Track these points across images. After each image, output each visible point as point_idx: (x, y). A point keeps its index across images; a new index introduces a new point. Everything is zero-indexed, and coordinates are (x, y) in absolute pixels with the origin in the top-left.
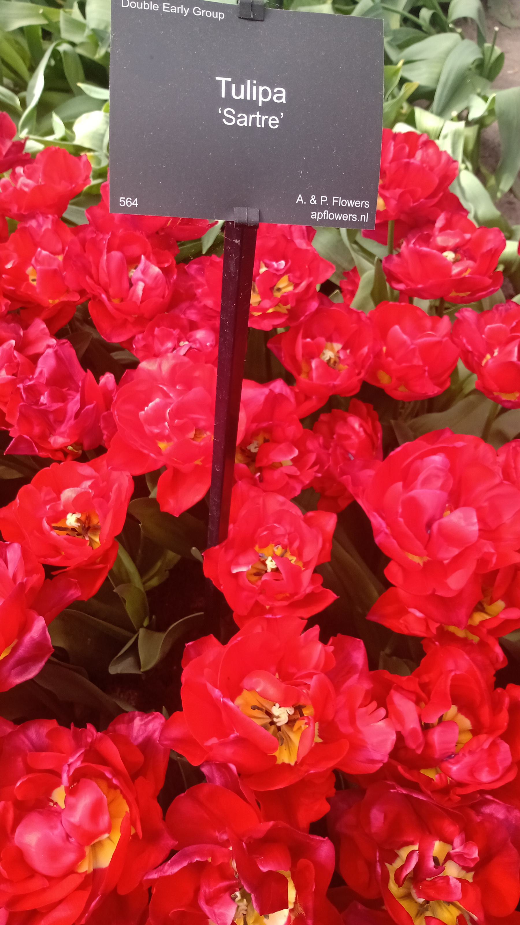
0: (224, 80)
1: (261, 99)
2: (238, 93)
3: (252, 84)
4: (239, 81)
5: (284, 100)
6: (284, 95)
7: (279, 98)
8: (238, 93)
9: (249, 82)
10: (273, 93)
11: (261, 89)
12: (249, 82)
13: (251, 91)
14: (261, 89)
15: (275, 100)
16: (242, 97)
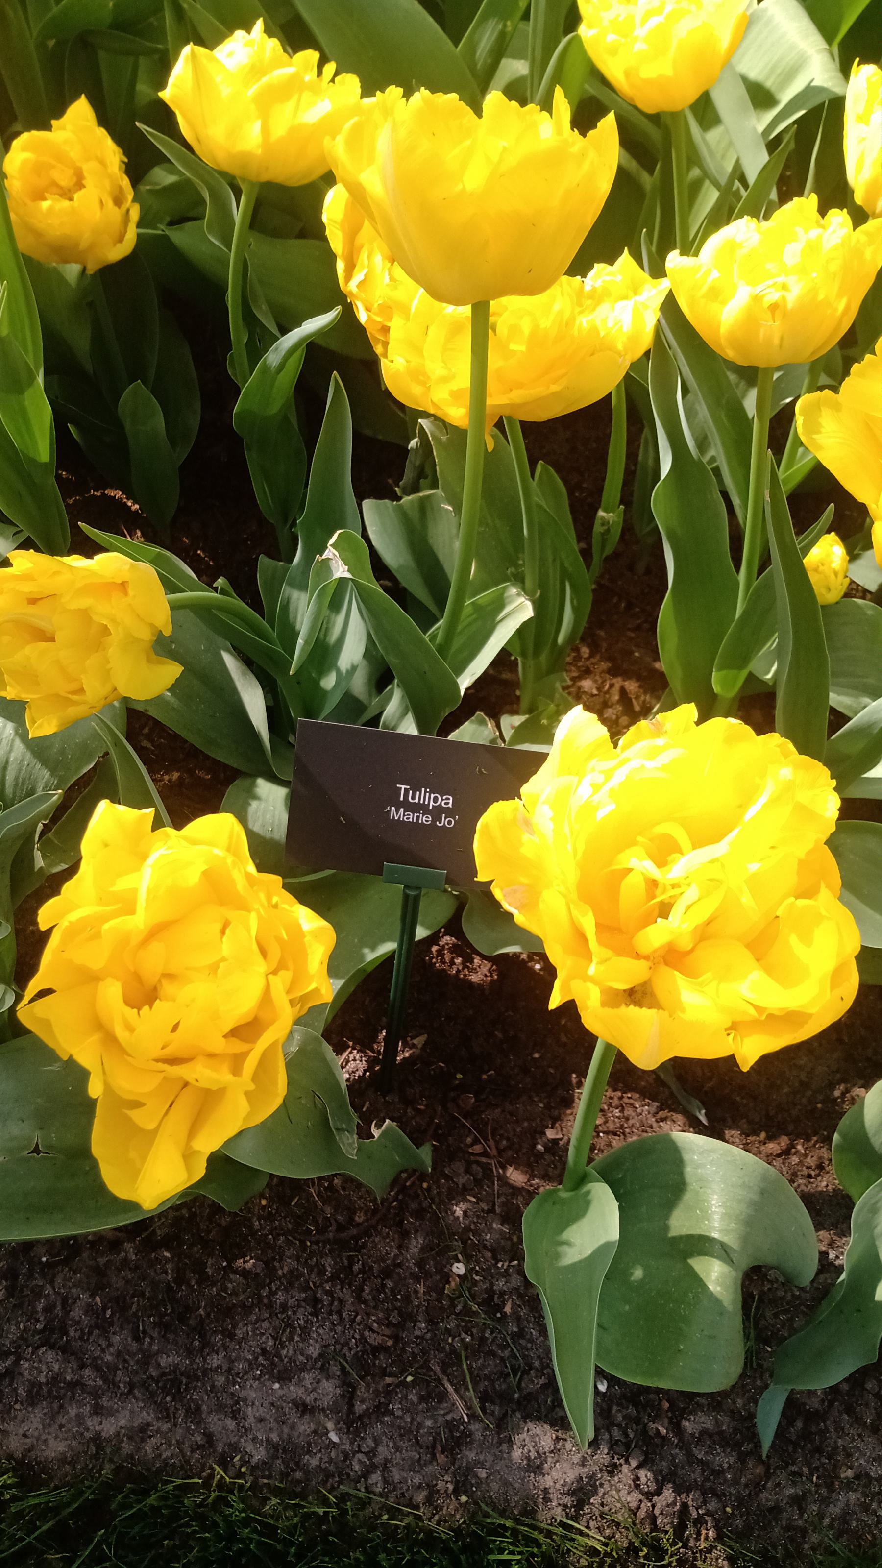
0: (403, 787)
1: (432, 803)
2: (413, 798)
3: (426, 792)
4: (416, 788)
5: (450, 805)
6: (451, 801)
7: (446, 804)
8: (413, 798)
9: (423, 789)
10: (442, 800)
11: (433, 796)
12: (423, 789)
13: (424, 797)
14: (433, 796)
15: (443, 804)
16: (417, 800)
